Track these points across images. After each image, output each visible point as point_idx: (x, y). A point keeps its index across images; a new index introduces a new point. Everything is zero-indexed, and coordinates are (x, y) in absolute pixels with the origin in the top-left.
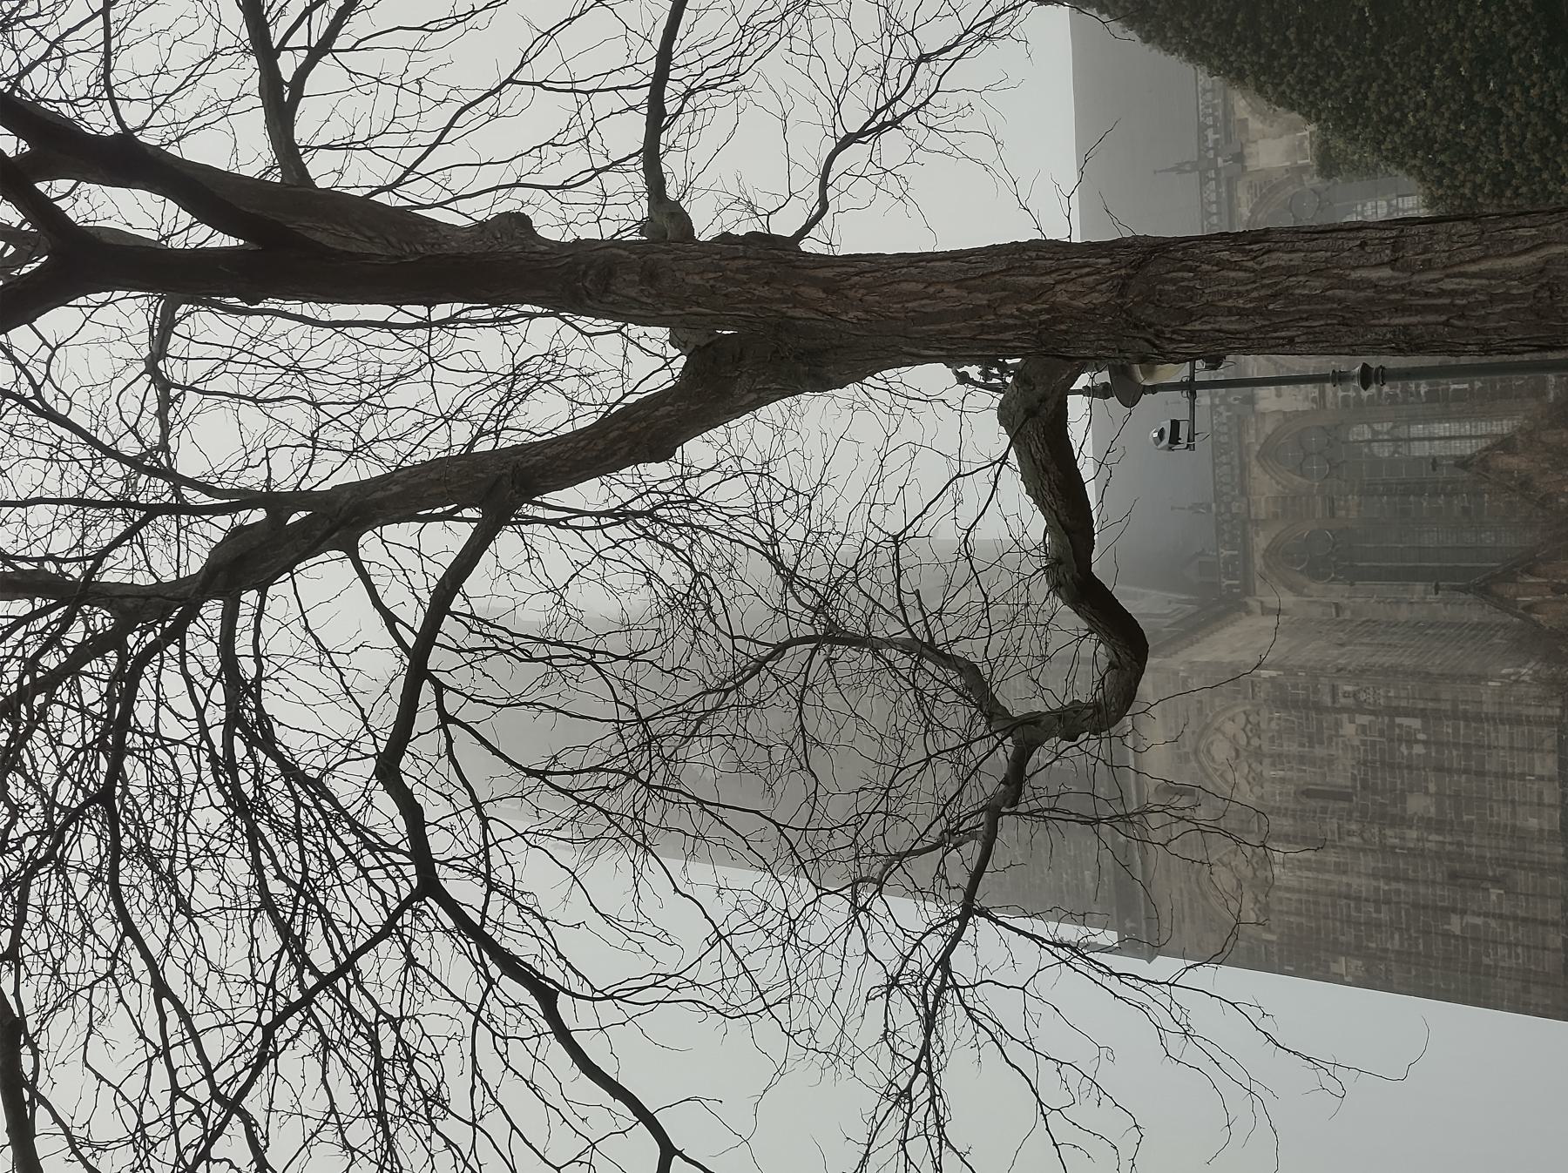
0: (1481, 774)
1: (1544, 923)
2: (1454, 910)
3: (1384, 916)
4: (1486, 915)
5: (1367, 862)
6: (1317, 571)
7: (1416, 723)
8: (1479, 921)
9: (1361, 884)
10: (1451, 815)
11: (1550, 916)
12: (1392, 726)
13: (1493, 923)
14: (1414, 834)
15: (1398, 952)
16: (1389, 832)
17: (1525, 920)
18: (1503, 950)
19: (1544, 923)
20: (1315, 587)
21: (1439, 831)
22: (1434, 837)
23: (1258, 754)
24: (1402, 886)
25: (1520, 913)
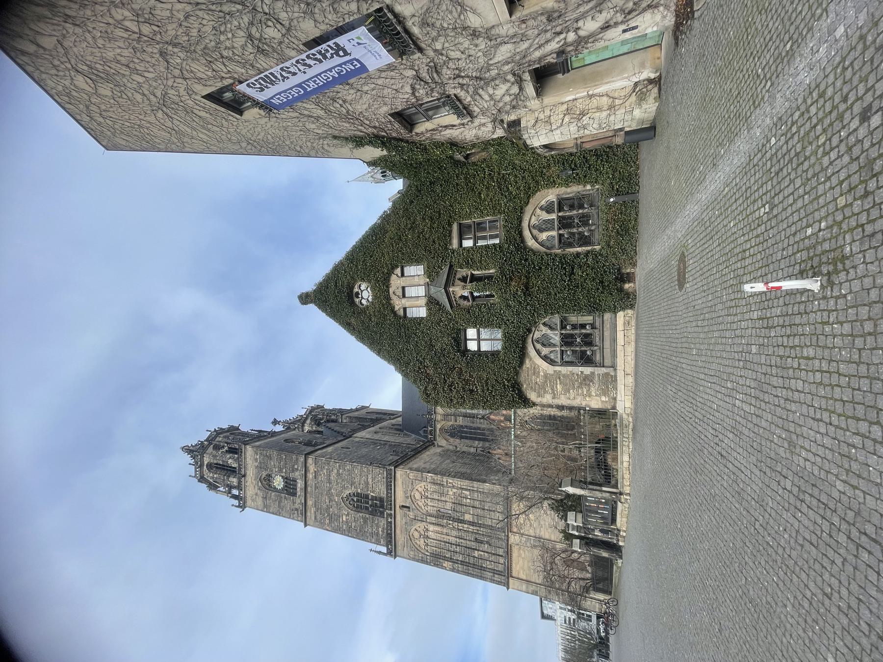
0: (484, 509)
1: (499, 555)
2: (476, 550)
3: (458, 550)
4: (484, 552)
5: (454, 533)
6: (452, 435)
7: (468, 493)
8: (482, 553)
9: (453, 540)
10: (476, 521)
11: (501, 554)
12: (462, 493)
13: (486, 554)
14: (466, 526)
15: (461, 561)
16: (460, 525)
17: (494, 554)
18: (488, 563)
19: (499, 555)
20: (451, 440)
21: (473, 525)
22: (471, 527)
23: (427, 498)
24: (463, 541)
25: (493, 552)
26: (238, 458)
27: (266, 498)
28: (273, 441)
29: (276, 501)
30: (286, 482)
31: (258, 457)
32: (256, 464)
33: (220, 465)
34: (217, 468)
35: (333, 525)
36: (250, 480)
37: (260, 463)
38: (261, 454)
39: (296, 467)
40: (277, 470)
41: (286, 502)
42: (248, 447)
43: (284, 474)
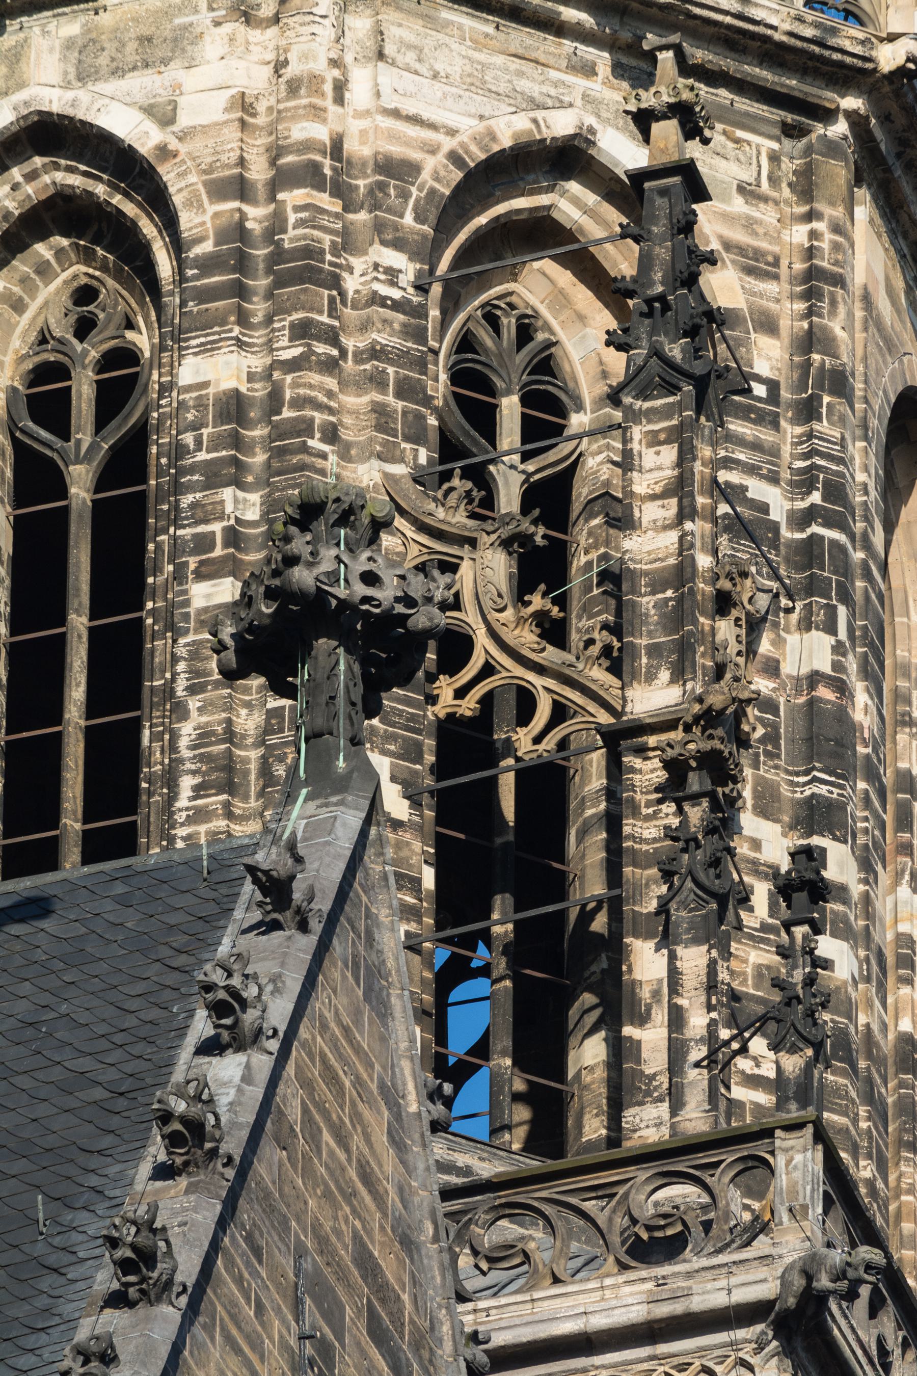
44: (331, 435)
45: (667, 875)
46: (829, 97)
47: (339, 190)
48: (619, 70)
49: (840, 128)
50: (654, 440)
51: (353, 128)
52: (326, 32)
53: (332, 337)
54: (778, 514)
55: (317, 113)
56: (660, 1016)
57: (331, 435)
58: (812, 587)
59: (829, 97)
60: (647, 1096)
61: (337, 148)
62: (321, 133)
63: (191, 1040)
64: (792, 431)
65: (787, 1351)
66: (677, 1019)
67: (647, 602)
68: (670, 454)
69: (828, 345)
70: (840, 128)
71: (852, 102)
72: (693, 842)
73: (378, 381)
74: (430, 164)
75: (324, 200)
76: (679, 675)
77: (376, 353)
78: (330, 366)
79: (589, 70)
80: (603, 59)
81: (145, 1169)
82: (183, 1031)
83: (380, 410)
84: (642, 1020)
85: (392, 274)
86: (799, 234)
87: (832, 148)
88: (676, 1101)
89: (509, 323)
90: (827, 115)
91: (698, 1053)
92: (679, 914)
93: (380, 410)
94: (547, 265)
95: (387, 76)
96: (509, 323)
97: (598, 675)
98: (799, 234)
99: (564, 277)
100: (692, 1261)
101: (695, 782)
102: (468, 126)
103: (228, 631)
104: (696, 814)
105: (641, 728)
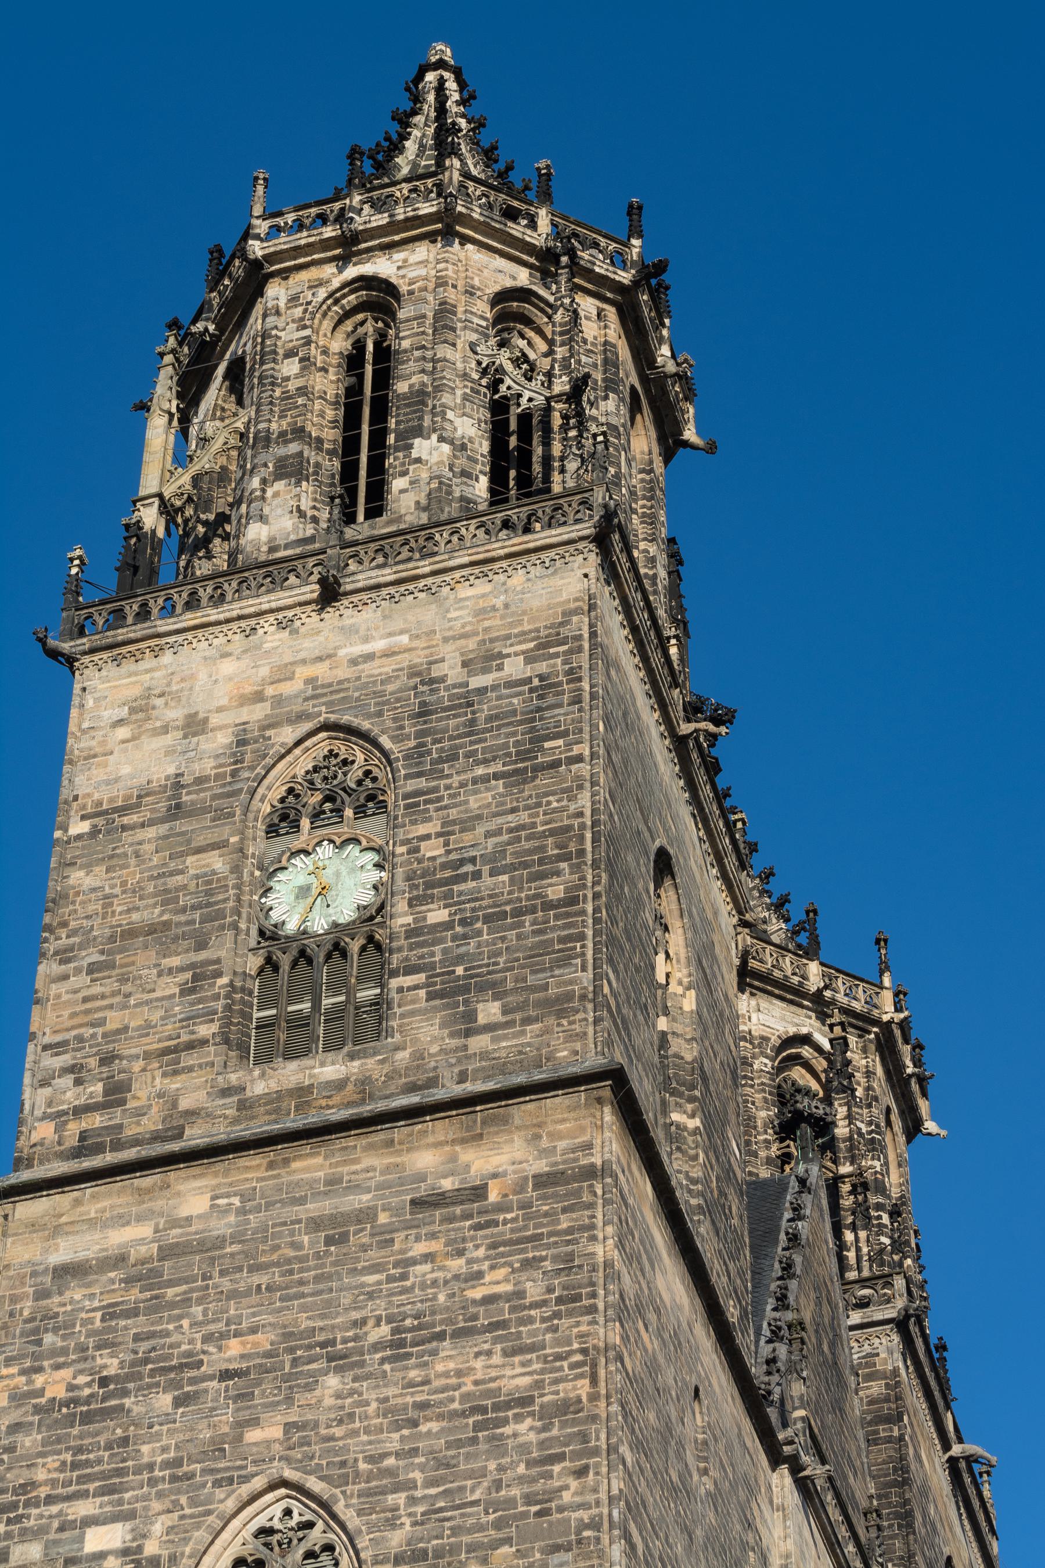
26: (468, 510)
27: (176, 811)
28: (645, 758)
29: (168, 898)
30: (338, 950)
31: (514, 668)
32: (451, 670)
33: (383, 379)
34: (354, 361)
35: (29, 1441)
36: (309, 646)
37: (468, 700)
38: (546, 686)
39: (489, 1011)
40: (432, 849)
41: (169, 986)
42: (591, 561)
43: (402, 918)
44: (753, 1103)
45: (853, 1213)
46: (870, 1028)
47: (751, 1043)
48: (817, 1018)
49: (872, 1036)
50: (840, 1105)
51: (753, 1028)
52: (745, 1004)
53: (752, 1079)
54: (864, 1131)
55: (745, 1024)
56: (853, 1249)
57: (753, 1103)
58: (874, 1149)
59: (870, 1028)
60: (851, 1270)
61: (750, 1032)
62: (746, 1029)
63: (785, 1219)
64: (866, 1111)
65: (899, 1332)
66: (858, 1249)
67: (842, 1145)
68: (845, 1109)
69: (873, 1090)
70: (872, 1036)
71: (875, 1029)
72: (860, 1205)
73: (764, 1091)
74: (773, 1038)
75: (748, 1045)
76: (852, 1164)
77: (763, 1084)
78: (752, 1086)
79: (810, 1018)
80: (813, 1015)
81: (780, 1249)
82: (781, 1218)
83: (765, 1098)
84: (849, 1250)
85: (766, 1065)
86: (864, 1062)
87: (870, 1041)
88: (859, 1269)
89: (789, 1082)
90: (869, 1033)
91: (866, 1258)
92: (858, 1223)
93: (765, 1098)
94: (798, 1067)
95: (761, 1016)
96: (789, 1082)
97: (829, 1164)
98: (864, 1062)
99: (803, 1071)
100: (872, 1308)
101: (859, 1190)
102: (782, 1029)
103: (776, 1123)
104: (860, 1198)
105: (843, 1176)
